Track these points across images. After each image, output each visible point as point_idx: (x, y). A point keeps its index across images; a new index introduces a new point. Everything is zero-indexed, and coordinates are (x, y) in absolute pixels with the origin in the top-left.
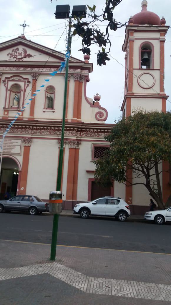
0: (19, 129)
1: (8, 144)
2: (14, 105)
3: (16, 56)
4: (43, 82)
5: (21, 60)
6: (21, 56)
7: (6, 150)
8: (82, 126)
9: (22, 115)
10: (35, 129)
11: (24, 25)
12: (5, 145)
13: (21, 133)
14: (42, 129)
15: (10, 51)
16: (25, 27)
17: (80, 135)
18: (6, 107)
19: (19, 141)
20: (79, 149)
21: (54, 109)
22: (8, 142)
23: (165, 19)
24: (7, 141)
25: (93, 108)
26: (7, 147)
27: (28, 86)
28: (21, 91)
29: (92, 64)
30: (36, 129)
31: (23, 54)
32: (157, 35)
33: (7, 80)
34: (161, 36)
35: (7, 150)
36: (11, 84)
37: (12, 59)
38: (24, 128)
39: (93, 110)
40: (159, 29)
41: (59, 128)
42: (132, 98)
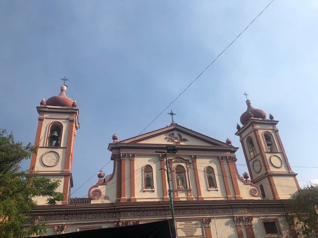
1: (189, 226)
2: (179, 185)
4: (202, 164)
5: (178, 144)
6: (178, 140)
7: (188, 233)
11: (172, 114)
17: (250, 212)
22: (189, 225)
25: (247, 186)
26: (189, 230)
30: (212, 208)
31: (179, 139)
32: (271, 127)
35: (190, 233)
36: (174, 165)
37: (169, 143)
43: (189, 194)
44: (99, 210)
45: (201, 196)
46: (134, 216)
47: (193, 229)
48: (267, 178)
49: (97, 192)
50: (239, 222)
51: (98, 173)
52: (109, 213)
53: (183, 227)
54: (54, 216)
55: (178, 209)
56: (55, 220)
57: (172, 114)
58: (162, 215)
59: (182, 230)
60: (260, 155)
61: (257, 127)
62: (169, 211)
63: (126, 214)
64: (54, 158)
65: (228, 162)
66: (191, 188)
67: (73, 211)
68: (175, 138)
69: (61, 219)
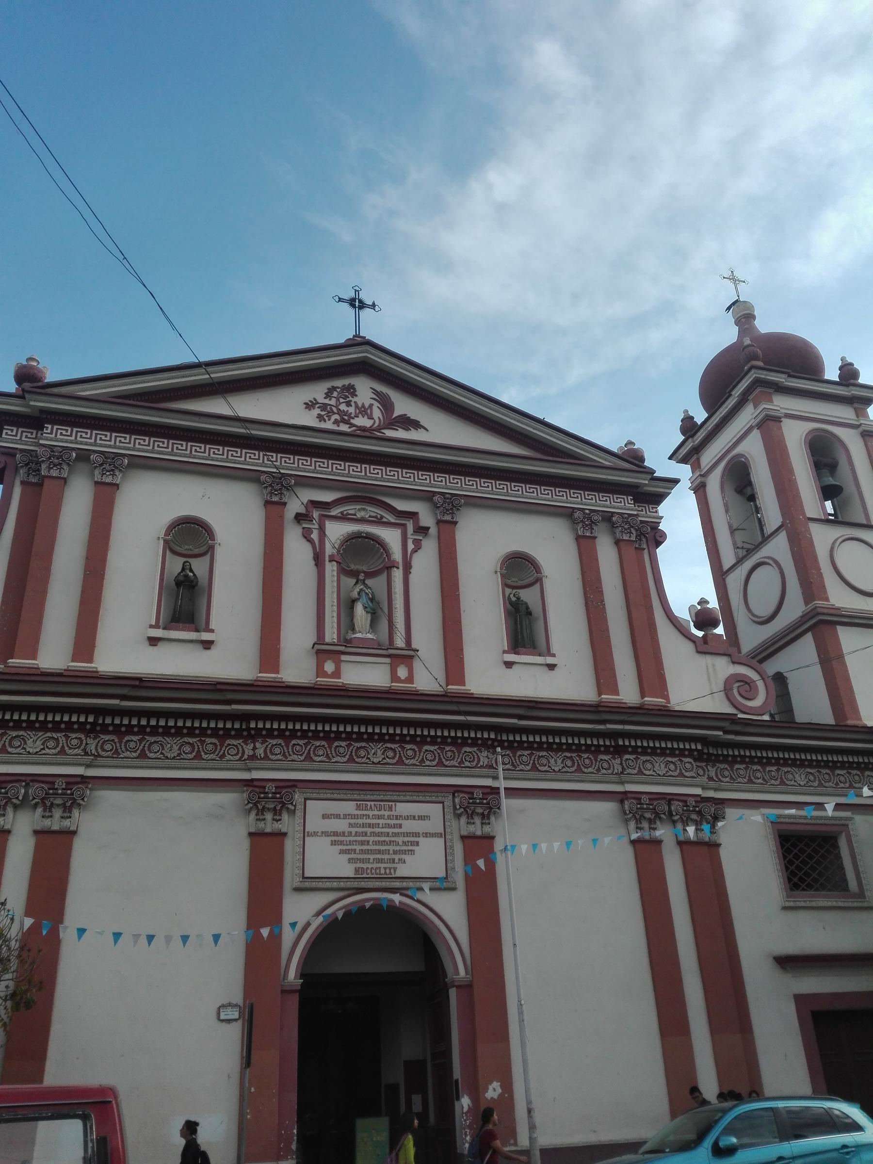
0: (426, 747)
2: (353, 629)
3: (346, 418)
6: (371, 417)
7: (368, 861)
8: (726, 732)
9: (410, 679)
11: (357, 304)
12: (366, 834)
13: (440, 764)
14: (540, 746)
15: (317, 391)
17: (710, 779)
18: (328, 639)
19: (434, 810)
20: (719, 845)
21: (554, 655)
23: (851, 364)
24: (371, 813)
25: (709, 659)
27: (418, 546)
31: (377, 413)
32: (845, 413)
33: (316, 514)
34: (858, 417)
36: (336, 531)
38: (454, 741)
39: (710, 667)
40: (853, 392)
42: (837, 627)
43: (402, 672)
46: (62, 752)
47: (400, 840)
48: (809, 637)
53: (341, 825)
55: (327, 737)
57: (357, 304)
58: (228, 757)
59: (334, 843)
60: (785, 531)
61: (782, 404)
62: (274, 742)
63: (16, 743)
65: (617, 542)
66: (413, 646)
68: (357, 406)
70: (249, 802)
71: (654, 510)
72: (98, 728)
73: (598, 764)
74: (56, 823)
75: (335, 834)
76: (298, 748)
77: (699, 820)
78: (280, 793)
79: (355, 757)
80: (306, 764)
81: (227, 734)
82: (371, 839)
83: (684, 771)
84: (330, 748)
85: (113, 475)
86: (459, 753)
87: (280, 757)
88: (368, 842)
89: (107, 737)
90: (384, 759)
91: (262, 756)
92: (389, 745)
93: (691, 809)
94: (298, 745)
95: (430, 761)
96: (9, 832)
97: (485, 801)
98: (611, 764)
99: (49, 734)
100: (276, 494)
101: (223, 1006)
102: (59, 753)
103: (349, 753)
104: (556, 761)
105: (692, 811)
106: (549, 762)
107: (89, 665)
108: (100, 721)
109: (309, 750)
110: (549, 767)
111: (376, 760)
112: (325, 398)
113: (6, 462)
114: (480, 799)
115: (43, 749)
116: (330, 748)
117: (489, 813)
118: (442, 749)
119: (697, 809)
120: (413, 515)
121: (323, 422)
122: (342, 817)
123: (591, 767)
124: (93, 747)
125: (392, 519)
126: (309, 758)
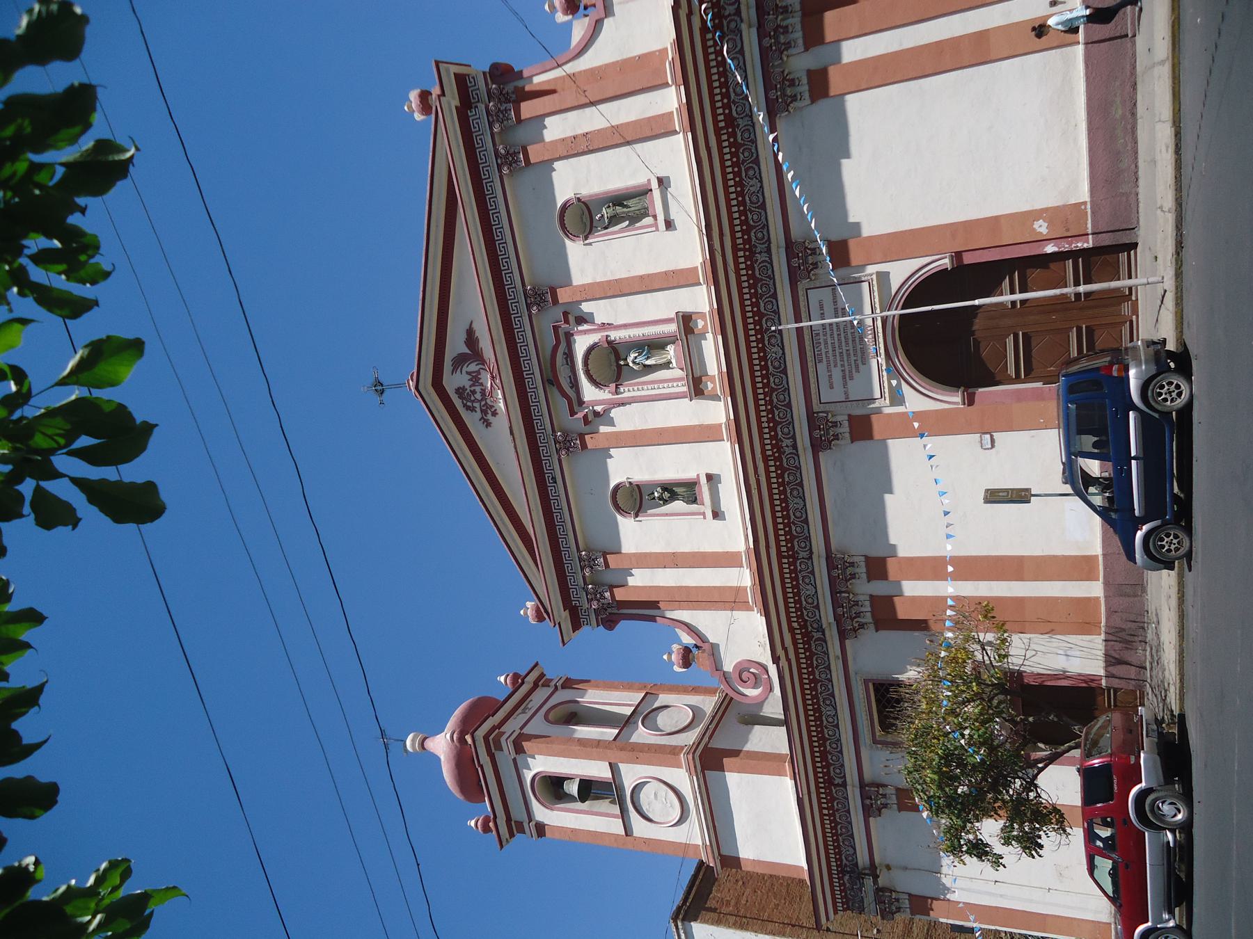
0: (762, 310)
6: (478, 372)
10: (750, 238)
15: (471, 420)
16: (384, 384)
17: (738, 12)
21: (649, 180)
24: (823, 351)
26: (847, 344)
27: (582, 319)
28: (610, 343)
29: (437, 63)
31: (473, 367)
41: (722, 124)
44: (803, 689)
45: (696, 268)
46: (812, 572)
49: (744, 679)
50: (792, 83)
51: (677, 669)
52: (812, 654)
53: (837, 374)
54: (838, 816)
56: (848, 811)
59: (851, 378)
62: (780, 433)
64: (653, 796)
66: (673, 315)
67: (815, 768)
68: (473, 385)
69: (844, 798)
70: (830, 448)
71: (472, 80)
72: (791, 553)
73: (746, 143)
74: (862, 570)
75: (844, 377)
76: (781, 415)
77: (782, 30)
78: (820, 426)
79: (781, 369)
80: (794, 409)
81: (780, 467)
82: (844, 348)
83: (737, 49)
84: (776, 390)
85: (597, 559)
86: (762, 280)
87: (791, 428)
88: (847, 350)
89: (796, 547)
90: (778, 345)
91: (791, 440)
92: (766, 342)
93: (773, 41)
94: (778, 415)
95: (773, 305)
96: (871, 596)
97: (800, 255)
98: (744, 128)
99: (801, 582)
100: (574, 444)
101: (982, 447)
102: (814, 575)
103: (778, 374)
104: (751, 186)
105: (774, 39)
106: (754, 192)
107: (743, 554)
108: (786, 554)
109: (782, 406)
110: (758, 192)
111: (781, 352)
112: (476, 411)
113: (607, 621)
114: (798, 260)
115: (811, 584)
116: (776, 390)
117: (809, 249)
118: (762, 296)
119: (772, 33)
120: (556, 328)
121: (497, 411)
122: (830, 374)
123: (750, 150)
124: (805, 553)
125: (563, 347)
126: (789, 405)
